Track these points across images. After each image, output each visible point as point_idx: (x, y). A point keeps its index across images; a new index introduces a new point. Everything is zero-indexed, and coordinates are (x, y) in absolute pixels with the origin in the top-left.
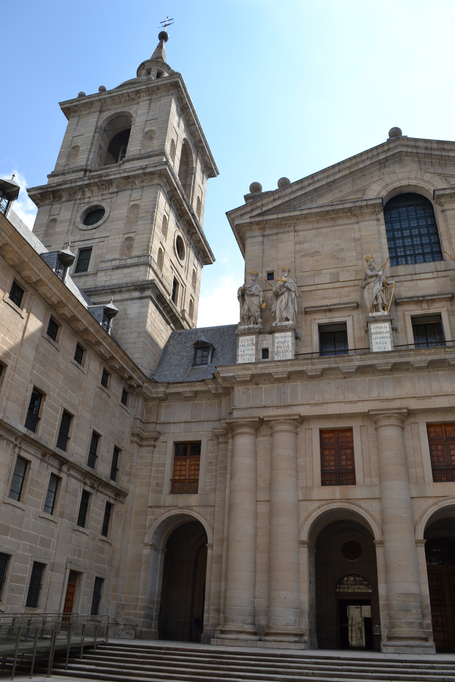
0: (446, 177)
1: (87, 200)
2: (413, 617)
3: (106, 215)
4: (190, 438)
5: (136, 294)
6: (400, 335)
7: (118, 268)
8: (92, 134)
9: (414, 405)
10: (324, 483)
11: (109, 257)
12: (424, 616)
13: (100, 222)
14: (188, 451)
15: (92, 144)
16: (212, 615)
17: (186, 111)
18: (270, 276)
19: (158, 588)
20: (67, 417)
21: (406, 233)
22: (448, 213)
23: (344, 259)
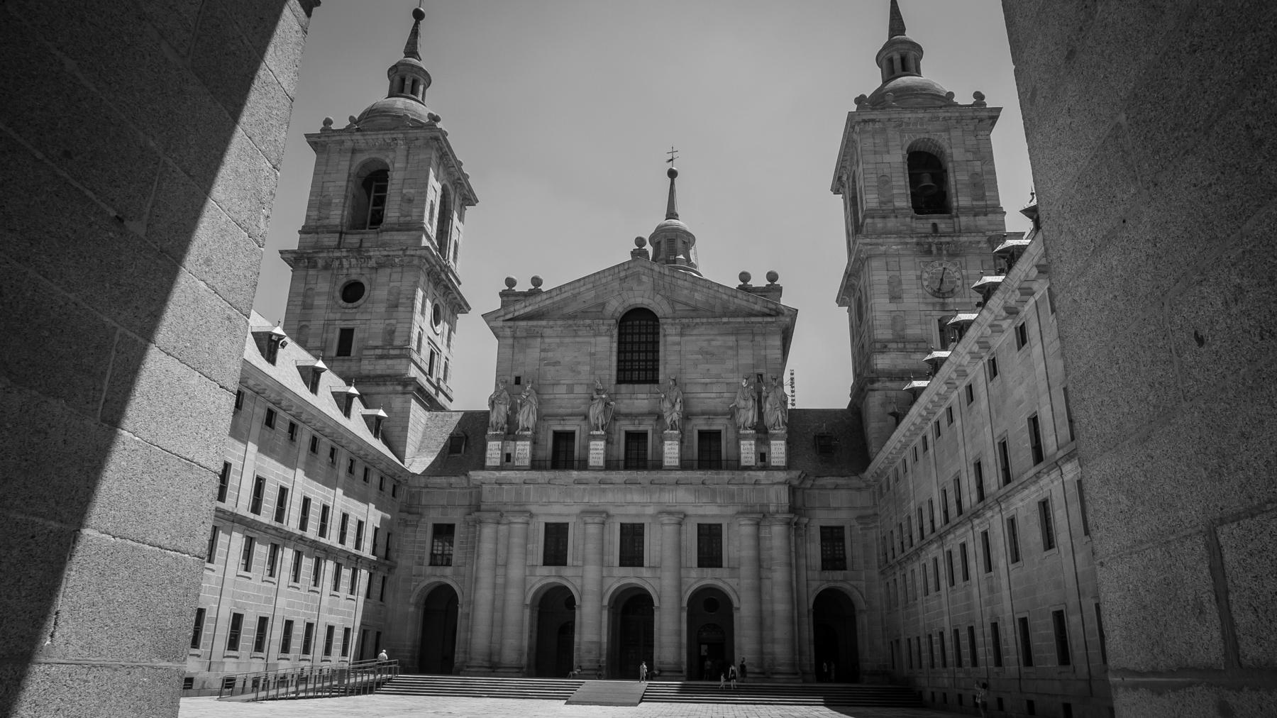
0: (672, 302)
1: (345, 271)
2: (593, 656)
3: (366, 293)
4: (446, 522)
5: (400, 388)
6: (615, 447)
7: (381, 357)
8: (344, 183)
9: (612, 511)
10: (545, 564)
11: (371, 343)
12: (601, 655)
13: (360, 301)
14: (444, 532)
15: (346, 197)
16: (461, 655)
17: (447, 161)
18: (518, 380)
19: (419, 635)
20: (360, 524)
21: (636, 348)
22: (669, 339)
23: (579, 373)
